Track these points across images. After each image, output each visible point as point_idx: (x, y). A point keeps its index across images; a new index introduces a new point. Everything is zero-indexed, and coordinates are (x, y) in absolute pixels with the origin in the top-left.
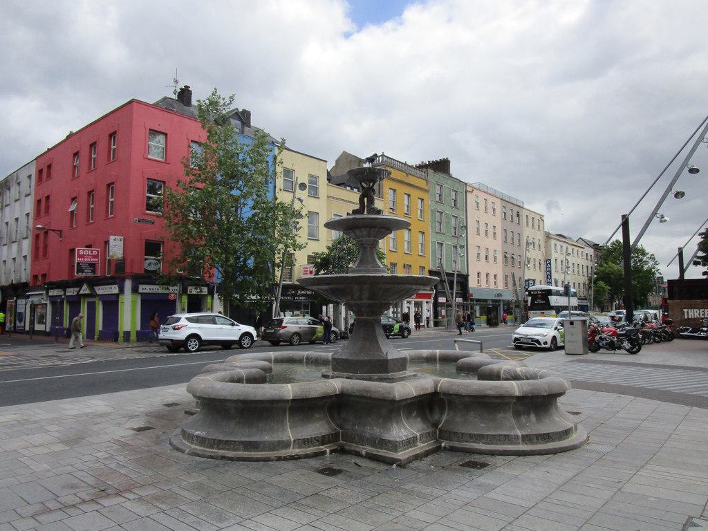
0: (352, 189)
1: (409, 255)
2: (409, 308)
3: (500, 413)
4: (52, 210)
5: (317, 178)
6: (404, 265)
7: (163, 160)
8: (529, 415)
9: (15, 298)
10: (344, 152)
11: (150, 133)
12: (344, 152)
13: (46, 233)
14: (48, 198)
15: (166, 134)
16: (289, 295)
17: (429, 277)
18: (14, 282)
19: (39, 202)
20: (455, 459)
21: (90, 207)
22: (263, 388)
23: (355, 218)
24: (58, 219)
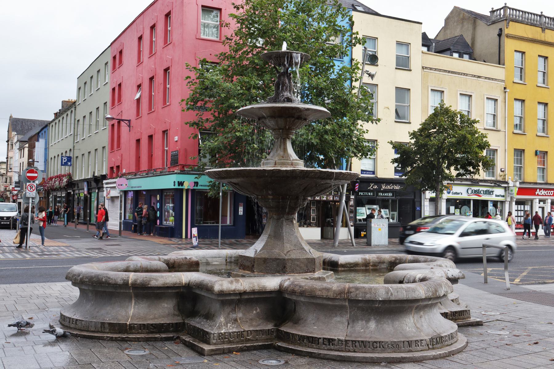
0: (461, 56)
1: (544, 139)
2: (543, 208)
3: (336, 316)
4: (123, 98)
5: (408, 45)
6: (536, 151)
7: (218, 39)
8: (368, 321)
9: (97, 191)
10: (455, 7)
11: (202, 10)
12: (455, 7)
13: (119, 123)
14: (120, 85)
15: (220, 10)
16: (369, 191)
17: (306, 169)
18: (96, 175)
19: (114, 89)
20: (304, 360)
21: (152, 95)
22: (162, 277)
23: (253, 108)
24: (128, 110)
